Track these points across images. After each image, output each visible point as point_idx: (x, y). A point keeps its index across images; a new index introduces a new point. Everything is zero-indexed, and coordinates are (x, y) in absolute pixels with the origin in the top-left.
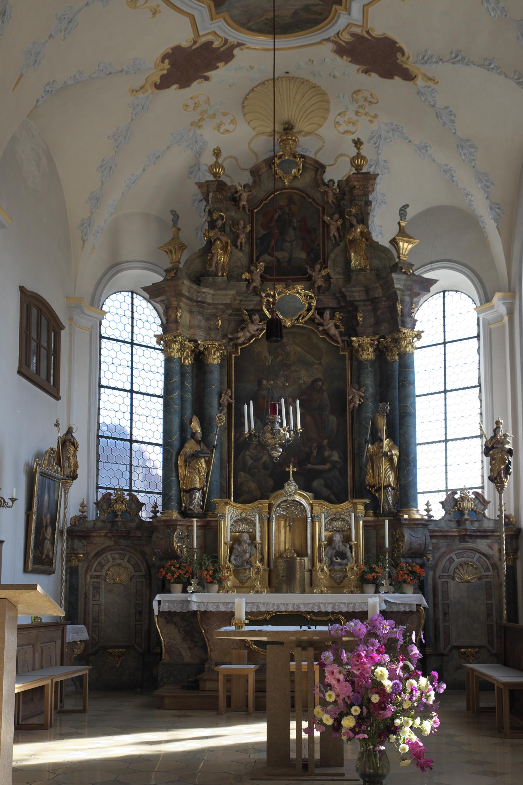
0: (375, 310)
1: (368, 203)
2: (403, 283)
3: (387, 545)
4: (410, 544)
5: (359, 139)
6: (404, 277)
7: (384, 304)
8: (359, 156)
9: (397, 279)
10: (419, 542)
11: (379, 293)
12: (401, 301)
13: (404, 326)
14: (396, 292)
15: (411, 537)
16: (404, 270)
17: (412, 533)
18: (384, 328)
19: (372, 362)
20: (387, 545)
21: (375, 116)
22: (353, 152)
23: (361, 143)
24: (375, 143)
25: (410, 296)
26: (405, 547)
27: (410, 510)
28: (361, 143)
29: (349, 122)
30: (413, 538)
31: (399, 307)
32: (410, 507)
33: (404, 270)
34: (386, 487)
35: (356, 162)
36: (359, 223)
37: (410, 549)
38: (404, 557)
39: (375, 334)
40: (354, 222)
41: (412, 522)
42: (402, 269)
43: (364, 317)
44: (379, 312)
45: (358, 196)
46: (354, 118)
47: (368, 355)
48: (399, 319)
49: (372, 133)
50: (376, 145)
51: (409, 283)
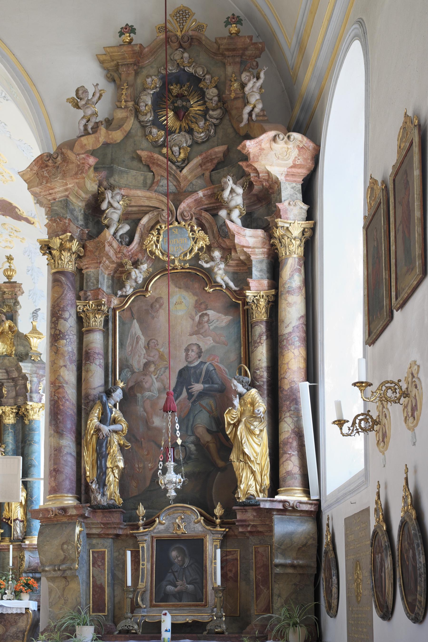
0: (15, 386)
1: (16, 303)
2: (29, 369)
3: (11, 564)
4: (29, 563)
5: (10, 256)
6: (30, 365)
7: (21, 382)
8: (10, 269)
9: (24, 366)
10: (36, 561)
11: (15, 375)
12: (30, 381)
13: (31, 400)
14: (25, 375)
15: (30, 558)
16: (33, 358)
17: (31, 555)
18: (20, 400)
19: (14, 425)
20: (11, 564)
21: (23, 239)
22: (7, 265)
23: (12, 259)
24: (29, 256)
25: (37, 377)
26: (25, 565)
27: (32, 537)
28: (12, 259)
29: (7, 241)
30: (32, 559)
31: (29, 386)
32: (32, 535)
33: (33, 358)
34: (15, 520)
35: (7, 274)
36: (7, 319)
37: (29, 567)
38: (25, 572)
39: (15, 405)
40: (4, 318)
41: (31, 547)
42: (31, 357)
43: (8, 391)
44: (18, 388)
45: (7, 299)
46: (9, 239)
47: (10, 420)
48: (28, 394)
49: (25, 249)
50: (30, 257)
51: (34, 369)
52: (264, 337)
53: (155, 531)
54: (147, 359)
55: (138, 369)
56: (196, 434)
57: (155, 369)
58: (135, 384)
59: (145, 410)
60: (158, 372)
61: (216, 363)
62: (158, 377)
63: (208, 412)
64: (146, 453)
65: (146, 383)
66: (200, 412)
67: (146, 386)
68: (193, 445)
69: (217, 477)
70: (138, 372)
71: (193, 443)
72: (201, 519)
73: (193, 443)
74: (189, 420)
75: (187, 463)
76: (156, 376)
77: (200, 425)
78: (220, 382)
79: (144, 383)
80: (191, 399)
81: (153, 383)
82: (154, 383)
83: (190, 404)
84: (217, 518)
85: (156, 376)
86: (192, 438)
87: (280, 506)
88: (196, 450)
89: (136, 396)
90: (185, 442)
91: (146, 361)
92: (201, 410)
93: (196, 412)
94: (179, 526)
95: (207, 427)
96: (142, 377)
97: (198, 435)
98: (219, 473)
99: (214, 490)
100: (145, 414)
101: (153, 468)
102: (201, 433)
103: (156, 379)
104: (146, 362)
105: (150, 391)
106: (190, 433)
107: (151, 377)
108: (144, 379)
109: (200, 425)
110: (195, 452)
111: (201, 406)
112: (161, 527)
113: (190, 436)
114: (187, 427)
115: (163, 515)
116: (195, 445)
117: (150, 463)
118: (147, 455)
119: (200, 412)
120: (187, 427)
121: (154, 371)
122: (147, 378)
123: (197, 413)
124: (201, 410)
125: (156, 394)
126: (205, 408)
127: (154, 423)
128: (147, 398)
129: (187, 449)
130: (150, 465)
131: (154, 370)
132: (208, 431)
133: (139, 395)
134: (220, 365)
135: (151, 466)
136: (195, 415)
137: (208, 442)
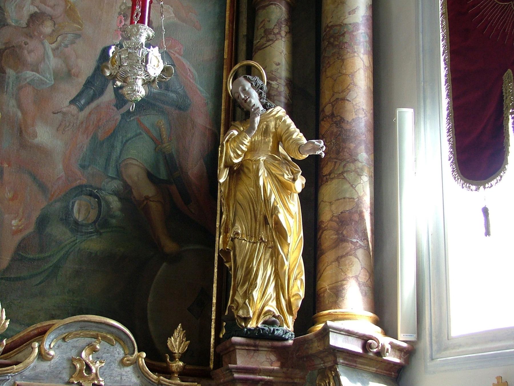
52: (284, 29)
53: (27, 373)
54: (37, 7)
55: (17, 22)
56: (125, 177)
57: (53, 31)
58: (6, 49)
59: (20, 106)
60: (59, 39)
61: (177, 55)
62: (57, 48)
63: (153, 139)
64: (10, 195)
65: (29, 52)
66: (137, 135)
67: (30, 58)
68: (116, 198)
69: (159, 273)
70: (15, 27)
71: (116, 193)
72: (139, 356)
73: (116, 193)
74: (113, 147)
75: (101, 234)
76: (54, 46)
77: (136, 163)
78: (180, 91)
79: (26, 52)
80: (120, 108)
81: (44, 57)
82: (48, 58)
83: (119, 117)
84: (173, 359)
85: (54, 46)
86: (115, 185)
87: (356, 347)
88: (122, 210)
89: (4, 72)
90: (101, 189)
91: (36, 10)
92: (140, 134)
93: (129, 135)
94: (89, 369)
95: (149, 170)
96: (23, 39)
97: (129, 182)
98: (165, 264)
99: (150, 299)
100: (20, 114)
101: (21, 231)
102: (136, 178)
103: (53, 50)
104: (36, 13)
105: (37, 71)
106: (112, 173)
107: (43, 44)
108: (26, 44)
109: (136, 163)
110: (118, 213)
111: (140, 124)
112: (45, 366)
113: (113, 178)
114: (108, 160)
115: (52, 337)
116: (121, 199)
117: (15, 218)
118: (12, 199)
119: (137, 135)
120: (108, 160)
121: (51, 35)
122: (33, 44)
123: (130, 139)
124: (140, 134)
125: (49, 79)
126: (147, 132)
127: (36, 137)
128: (29, 84)
129: (103, 203)
130: (13, 222)
131: (52, 33)
132: (151, 177)
133: (10, 72)
134: (184, 61)
135: (18, 226)
136: (127, 141)
137: (147, 198)
